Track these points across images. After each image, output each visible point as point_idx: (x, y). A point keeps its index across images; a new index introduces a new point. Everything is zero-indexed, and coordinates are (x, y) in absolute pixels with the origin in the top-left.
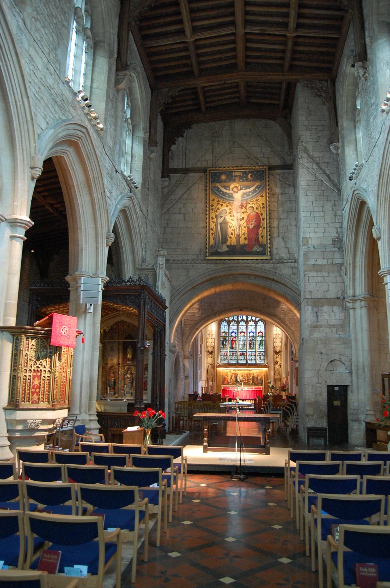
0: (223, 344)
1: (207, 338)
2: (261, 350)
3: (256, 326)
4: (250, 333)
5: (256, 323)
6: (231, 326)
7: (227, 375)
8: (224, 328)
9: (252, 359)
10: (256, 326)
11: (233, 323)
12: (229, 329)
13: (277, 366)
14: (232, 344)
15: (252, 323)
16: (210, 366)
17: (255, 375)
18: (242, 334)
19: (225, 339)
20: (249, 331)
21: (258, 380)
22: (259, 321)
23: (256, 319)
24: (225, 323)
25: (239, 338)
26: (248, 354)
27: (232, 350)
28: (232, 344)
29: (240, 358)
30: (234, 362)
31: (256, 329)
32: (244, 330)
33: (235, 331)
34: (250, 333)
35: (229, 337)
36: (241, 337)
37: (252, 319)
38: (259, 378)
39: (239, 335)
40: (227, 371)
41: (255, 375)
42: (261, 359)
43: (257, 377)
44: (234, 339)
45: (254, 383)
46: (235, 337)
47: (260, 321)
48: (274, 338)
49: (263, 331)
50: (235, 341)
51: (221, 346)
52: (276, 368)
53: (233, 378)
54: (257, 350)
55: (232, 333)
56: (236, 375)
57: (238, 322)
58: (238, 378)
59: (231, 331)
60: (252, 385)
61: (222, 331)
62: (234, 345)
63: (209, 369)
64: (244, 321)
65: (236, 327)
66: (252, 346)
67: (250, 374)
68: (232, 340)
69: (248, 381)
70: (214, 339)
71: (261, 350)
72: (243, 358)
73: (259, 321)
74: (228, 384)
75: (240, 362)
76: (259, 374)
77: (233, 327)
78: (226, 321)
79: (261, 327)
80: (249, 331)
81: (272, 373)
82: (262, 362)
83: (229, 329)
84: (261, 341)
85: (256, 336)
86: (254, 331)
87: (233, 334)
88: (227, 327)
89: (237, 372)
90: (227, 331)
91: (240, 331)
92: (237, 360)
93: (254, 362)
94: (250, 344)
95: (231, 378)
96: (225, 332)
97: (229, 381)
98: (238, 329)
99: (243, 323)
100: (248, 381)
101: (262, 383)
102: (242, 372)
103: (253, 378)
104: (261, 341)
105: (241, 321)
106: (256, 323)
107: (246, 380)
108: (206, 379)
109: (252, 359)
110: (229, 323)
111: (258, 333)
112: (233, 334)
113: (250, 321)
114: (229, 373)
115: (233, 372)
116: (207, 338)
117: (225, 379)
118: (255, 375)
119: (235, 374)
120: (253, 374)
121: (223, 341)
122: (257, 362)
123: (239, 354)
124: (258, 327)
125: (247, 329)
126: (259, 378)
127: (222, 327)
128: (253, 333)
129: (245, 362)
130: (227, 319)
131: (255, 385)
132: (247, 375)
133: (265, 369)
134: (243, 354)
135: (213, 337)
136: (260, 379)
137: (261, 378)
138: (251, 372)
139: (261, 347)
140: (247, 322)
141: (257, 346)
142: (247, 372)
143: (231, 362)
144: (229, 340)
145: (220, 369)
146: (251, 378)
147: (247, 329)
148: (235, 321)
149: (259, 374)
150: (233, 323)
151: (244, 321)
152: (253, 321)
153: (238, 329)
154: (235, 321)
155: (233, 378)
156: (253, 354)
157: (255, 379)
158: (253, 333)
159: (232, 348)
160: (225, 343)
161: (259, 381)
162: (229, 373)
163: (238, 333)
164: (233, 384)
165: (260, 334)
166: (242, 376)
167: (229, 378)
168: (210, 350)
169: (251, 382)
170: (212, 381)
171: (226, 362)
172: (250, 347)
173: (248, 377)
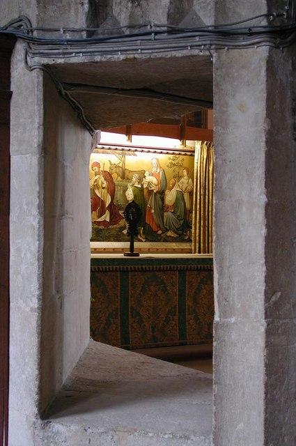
17: (152, 180)
21: (163, 208)
38: (170, 197)
41: (149, 178)
43: (162, 193)
67: (125, 175)
76: (169, 171)
101: (187, 226)
103: (140, 192)
118: (149, 178)
120: (142, 175)
126: (170, 197)
132: (108, 176)
136: (176, 205)
137: (180, 196)
157: (151, 203)
161: (168, 215)
173: (112, 193)
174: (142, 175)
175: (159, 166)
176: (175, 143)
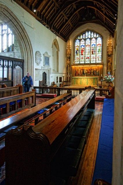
0: (77, 53)
1: (67, 50)
2: (99, 55)
3: (96, 40)
4: (92, 45)
5: (96, 38)
6: (81, 42)
7: (78, 70)
8: (77, 43)
9: (93, 61)
10: (96, 40)
11: (83, 40)
12: (80, 44)
13: (109, 64)
14: (82, 53)
15: (94, 39)
16: (68, 65)
18: (88, 46)
19: (78, 50)
20: (92, 44)
22: (98, 37)
23: (97, 35)
24: (78, 41)
25: (86, 48)
26: (91, 57)
27: (82, 56)
28: (82, 53)
29: (86, 60)
30: (83, 62)
31: (96, 42)
32: (89, 44)
33: (84, 45)
34: (92, 45)
35: (80, 48)
36: (87, 48)
37: (94, 37)
38: (97, 71)
39: (86, 47)
40: (78, 68)
42: (99, 60)
43: (96, 71)
44: (83, 50)
45: (94, 75)
46: (84, 49)
47: (99, 38)
48: (107, 47)
49: (101, 43)
50: (83, 51)
51: (76, 54)
52: (108, 66)
53: (82, 71)
54: (97, 55)
55: (82, 46)
56: (83, 70)
57: (85, 40)
58: (84, 71)
59: (81, 45)
60: (93, 75)
61: (76, 45)
62: (83, 53)
63: (68, 67)
64: (89, 38)
65: (84, 42)
66: (94, 53)
67: (92, 69)
68: (82, 50)
69: (90, 73)
70: (71, 50)
71: (99, 55)
72: (88, 60)
73: (98, 37)
74: (78, 75)
75: (86, 62)
76: (97, 69)
77: (83, 42)
78: (78, 39)
79: (99, 40)
80: (92, 44)
81: (105, 68)
82: (100, 62)
83: (80, 44)
84: (99, 49)
85: (96, 47)
86: (95, 44)
87: (82, 47)
88: (79, 43)
89: (84, 68)
90: (79, 45)
91: (86, 44)
92: (85, 61)
93: (95, 62)
94: (93, 52)
95: (80, 72)
96: (78, 46)
97: (79, 73)
98: (85, 43)
99: (88, 40)
100: (90, 73)
102: (87, 68)
103: (93, 71)
104: (99, 49)
105: (87, 39)
106: (96, 38)
107: (88, 72)
108: (66, 72)
109: (93, 61)
110: (80, 40)
111: (98, 45)
112: (82, 47)
113: (93, 38)
114: (79, 69)
115: (81, 68)
116: (67, 50)
117: (77, 72)
119: (83, 69)
120: (94, 69)
121: (77, 52)
122: (97, 62)
123: (86, 57)
124: (97, 41)
125: (91, 43)
126: (97, 71)
127: (76, 43)
128: (95, 45)
129: (89, 62)
130: (79, 38)
131: (95, 75)
132: (90, 70)
133: (101, 66)
134: (88, 58)
135: (71, 49)
138: (92, 68)
139: (99, 53)
140: (91, 39)
141: (97, 53)
142: (89, 68)
143: (81, 63)
144: (80, 51)
145: (73, 67)
146: (92, 71)
147: (91, 43)
148: (84, 39)
149: (97, 69)
150: (83, 40)
151: (89, 38)
152: (95, 38)
153: (85, 43)
154: (84, 39)
155: (81, 72)
156: (94, 58)
158: (95, 45)
159: (82, 55)
160: (77, 52)
162: (79, 69)
163: (85, 46)
164: (81, 75)
165: (99, 45)
166: (87, 71)
167: (79, 72)
168: (68, 56)
169: (92, 74)
170: (70, 75)
171: (78, 63)
172: (92, 54)
174: (94, 69)
175: (96, 68)
176: (96, 66)
